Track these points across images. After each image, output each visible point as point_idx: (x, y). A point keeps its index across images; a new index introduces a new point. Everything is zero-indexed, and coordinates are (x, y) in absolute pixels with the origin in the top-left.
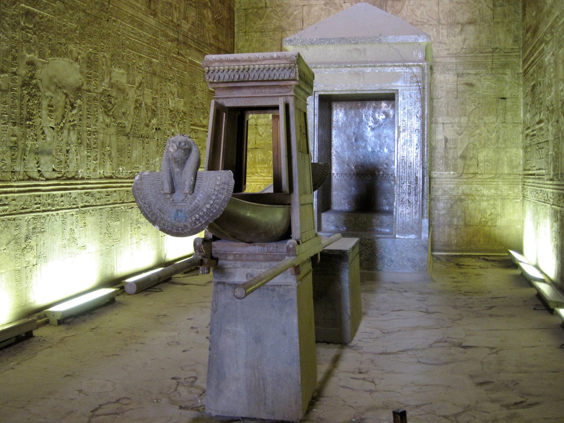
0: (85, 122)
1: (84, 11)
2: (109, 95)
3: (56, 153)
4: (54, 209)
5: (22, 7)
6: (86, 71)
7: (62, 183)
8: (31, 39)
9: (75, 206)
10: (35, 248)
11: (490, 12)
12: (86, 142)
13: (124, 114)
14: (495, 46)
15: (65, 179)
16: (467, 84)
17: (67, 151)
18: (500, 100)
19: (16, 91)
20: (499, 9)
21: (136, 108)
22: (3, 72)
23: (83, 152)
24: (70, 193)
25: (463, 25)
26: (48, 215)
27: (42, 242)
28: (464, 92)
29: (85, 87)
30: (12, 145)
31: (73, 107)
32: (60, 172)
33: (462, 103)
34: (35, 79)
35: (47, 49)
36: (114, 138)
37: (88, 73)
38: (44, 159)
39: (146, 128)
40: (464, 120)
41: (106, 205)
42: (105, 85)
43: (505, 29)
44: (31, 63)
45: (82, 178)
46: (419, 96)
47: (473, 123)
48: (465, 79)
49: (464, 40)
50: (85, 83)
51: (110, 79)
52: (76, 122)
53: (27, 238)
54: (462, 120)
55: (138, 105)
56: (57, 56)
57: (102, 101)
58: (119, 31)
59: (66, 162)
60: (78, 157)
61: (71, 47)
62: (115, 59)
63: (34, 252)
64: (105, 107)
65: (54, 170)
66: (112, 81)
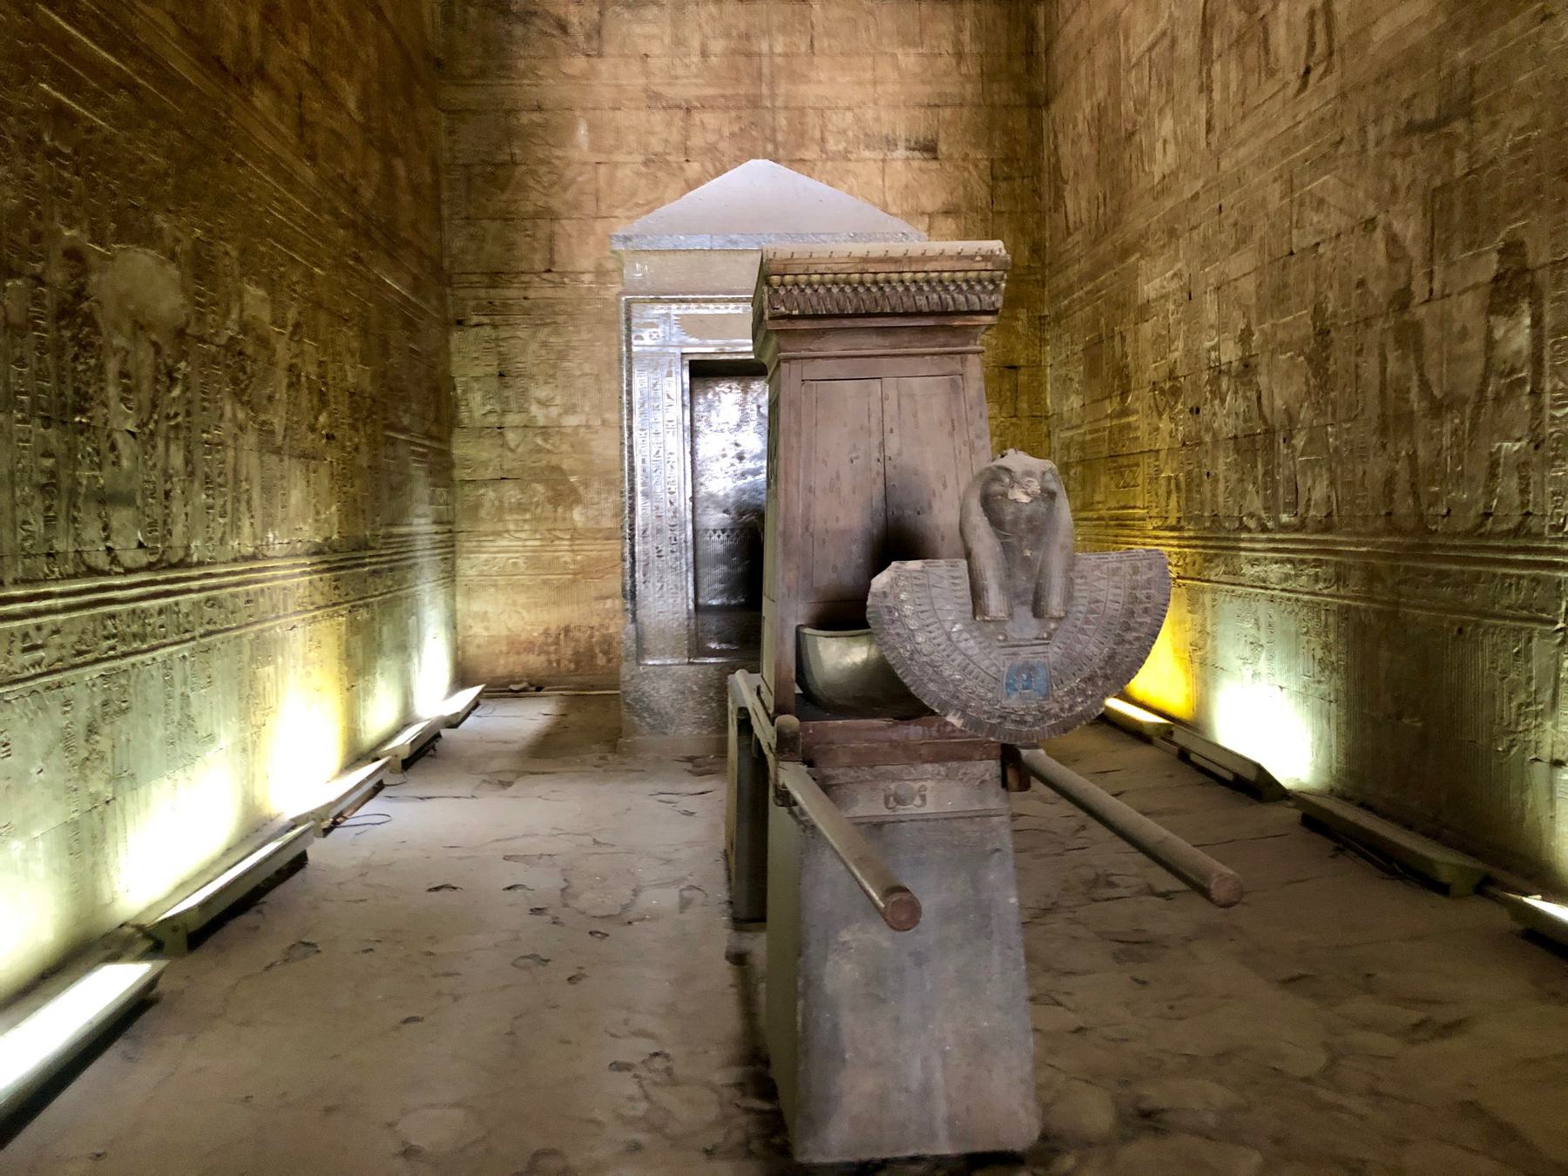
0: (196, 419)
1: (180, 129)
3: (144, 498)
4: (145, 646)
5: (46, 95)
7: (160, 577)
9: (187, 636)
10: (109, 755)
15: (164, 568)
17: (167, 494)
19: (45, 331)
20: (1003, 185)
21: (291, 385)
22: (12, 274)
23: (199, 495)
24: (177, 604)
25: (930, 215)
26: (133, 665)
27: (123, 739)
30: (44, 480)
31: (173, 381)
32: (153, 551)
37: (197, 294)
38: (120, 517)
39: (311, 436)
41: (248, 625)
50: (193, 322)
51: (242, 311)
52: (180, 419)
53: (91, 730)
57: (228, 366)
59: (165, 523)
61: (159, 219)
62: (250, 265)
63: (107, 767)
65: (141, 545)
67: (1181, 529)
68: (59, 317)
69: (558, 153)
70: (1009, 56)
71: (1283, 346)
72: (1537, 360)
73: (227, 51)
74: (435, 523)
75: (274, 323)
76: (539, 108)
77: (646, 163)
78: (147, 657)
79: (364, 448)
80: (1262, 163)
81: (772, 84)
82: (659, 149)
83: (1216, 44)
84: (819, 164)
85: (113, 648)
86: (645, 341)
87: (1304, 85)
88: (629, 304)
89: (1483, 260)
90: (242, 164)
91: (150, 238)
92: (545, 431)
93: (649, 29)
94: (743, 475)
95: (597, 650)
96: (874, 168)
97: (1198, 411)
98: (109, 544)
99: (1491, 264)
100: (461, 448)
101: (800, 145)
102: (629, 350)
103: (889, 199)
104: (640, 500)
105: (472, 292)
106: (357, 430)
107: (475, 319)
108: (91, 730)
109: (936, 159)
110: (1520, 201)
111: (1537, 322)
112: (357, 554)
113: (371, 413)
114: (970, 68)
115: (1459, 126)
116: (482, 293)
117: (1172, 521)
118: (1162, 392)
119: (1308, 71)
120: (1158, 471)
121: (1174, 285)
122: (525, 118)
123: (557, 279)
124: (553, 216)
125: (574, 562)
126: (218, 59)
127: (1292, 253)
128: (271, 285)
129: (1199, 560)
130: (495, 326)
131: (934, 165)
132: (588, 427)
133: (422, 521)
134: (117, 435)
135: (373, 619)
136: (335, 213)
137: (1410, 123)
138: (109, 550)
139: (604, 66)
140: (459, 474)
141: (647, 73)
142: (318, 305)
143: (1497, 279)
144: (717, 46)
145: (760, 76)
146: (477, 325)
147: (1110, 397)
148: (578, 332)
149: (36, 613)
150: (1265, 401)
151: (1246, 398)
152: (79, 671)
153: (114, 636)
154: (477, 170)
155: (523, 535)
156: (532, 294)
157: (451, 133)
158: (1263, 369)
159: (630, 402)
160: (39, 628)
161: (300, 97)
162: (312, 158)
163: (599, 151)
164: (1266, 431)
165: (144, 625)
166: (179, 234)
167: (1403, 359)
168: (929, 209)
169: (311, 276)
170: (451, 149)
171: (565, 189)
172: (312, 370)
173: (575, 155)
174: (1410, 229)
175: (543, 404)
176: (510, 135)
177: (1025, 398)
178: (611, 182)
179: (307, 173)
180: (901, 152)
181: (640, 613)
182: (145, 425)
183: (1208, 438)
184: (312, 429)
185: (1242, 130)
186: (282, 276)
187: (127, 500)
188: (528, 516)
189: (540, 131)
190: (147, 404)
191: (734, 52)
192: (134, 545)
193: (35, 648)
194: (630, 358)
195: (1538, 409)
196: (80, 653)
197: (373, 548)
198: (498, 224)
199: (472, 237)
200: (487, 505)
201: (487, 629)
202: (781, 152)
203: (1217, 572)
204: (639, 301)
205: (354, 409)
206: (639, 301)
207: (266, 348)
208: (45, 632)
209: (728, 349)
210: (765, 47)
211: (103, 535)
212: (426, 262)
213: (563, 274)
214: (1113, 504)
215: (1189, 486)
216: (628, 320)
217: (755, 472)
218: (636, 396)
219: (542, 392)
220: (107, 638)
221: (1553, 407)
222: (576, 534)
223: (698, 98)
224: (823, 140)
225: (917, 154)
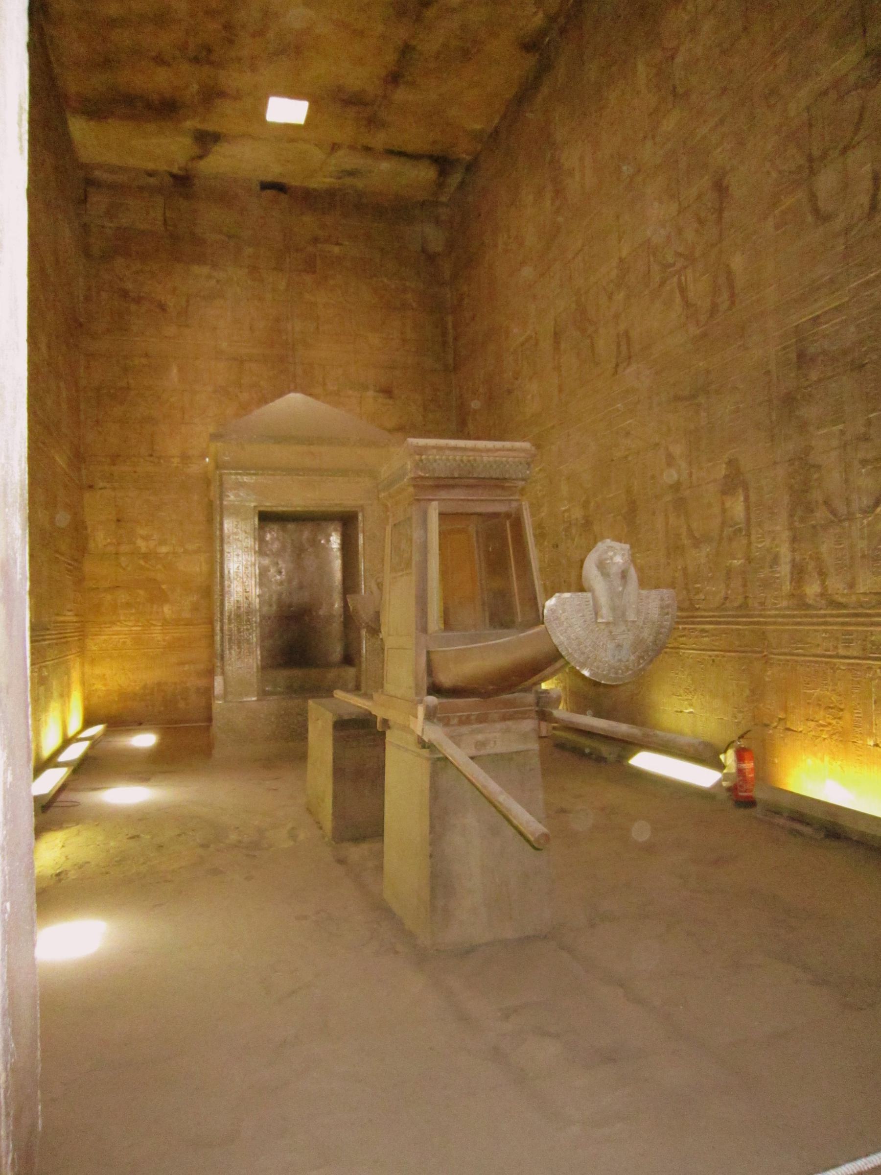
11: (421, 418)
72: (748, 520)
74: (76, 615)
76: (147, 355)
83: (563, 346)
86: (231, 497)
88: (221, 476)
92: (146, 557)
94: (281, 583)
95: (179, 697)
97: (557, 546)
100: (89, 567)
102: (221, 504)
107: (101, 485)
109: (391, 397)
119: (617, 365)
122: (137, 362)
125: (164, 640)
127: (612, 460)
130: (114, 489)
131: (391, 402)
132: (174, 553)
133: (70, 613)
143: (726, 476)
146: (101, 489)
155: (130, 624)
175: (146, 538)
180: (371, 393)
181: (228, 668)
188: (133, 611)
195: (750, 543)
197: (48, 629)
201: (105, 685)
204: (227, 474)
206: (227, 474)
209: (283, 503)
213: (159, 458)
217: (290, 581)
219: (142, 532)
222: (165, 623)
224: (325, 384)
225: (381, 395)
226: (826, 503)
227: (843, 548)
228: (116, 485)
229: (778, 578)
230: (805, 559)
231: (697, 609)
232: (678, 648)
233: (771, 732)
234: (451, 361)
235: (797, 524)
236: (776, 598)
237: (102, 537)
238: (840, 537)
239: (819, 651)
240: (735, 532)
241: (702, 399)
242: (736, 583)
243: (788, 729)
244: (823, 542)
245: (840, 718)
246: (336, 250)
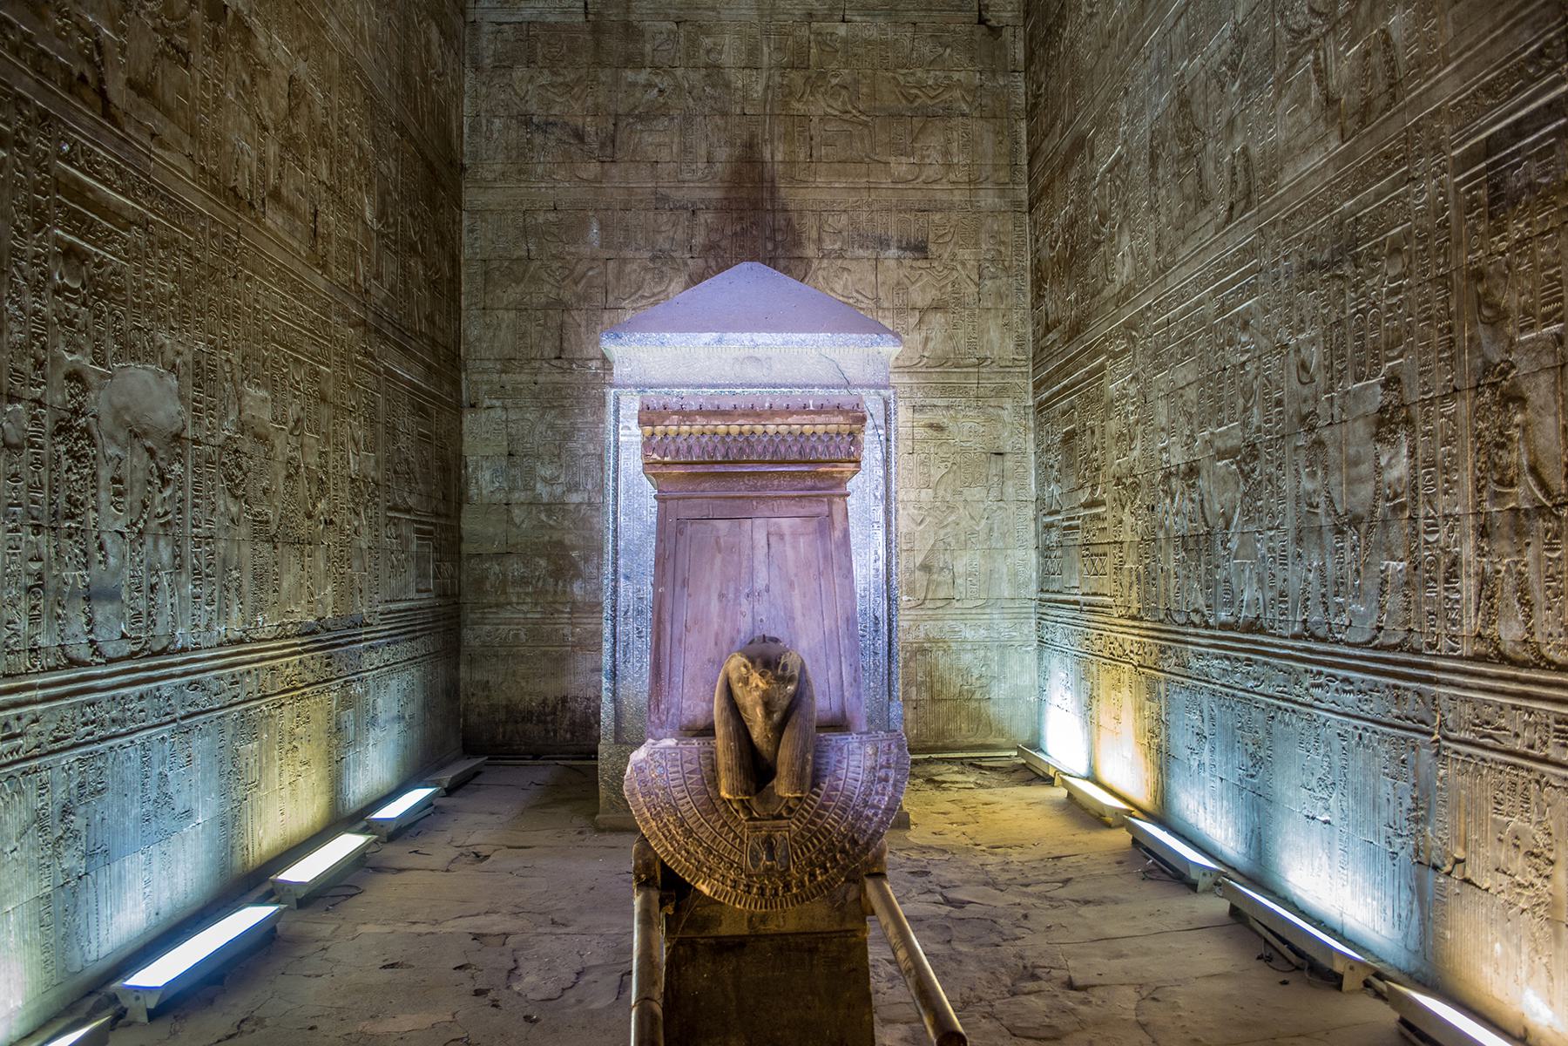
2: (236, 451)
6: (192, 394)
8: (76, 316)
9: (168, 718)
11: (973, 289)
12: (191, 561)
13: (265, 491)
14: (982, 355)
16: (931, 426)
17: (152, 588)
18: (994, 458)
20: (989, 283)
21: (289, 476)
23: (184, 585)
28: (924, 441)
29: (189, 433)
31: (165, 483)
33: (922, 463)
34: (84, 414)
35: (110, 342)
36: (246, 550)
39: (307, 523)
40: (926, 495)
41: (231, 705)
42: (228, 428)
43: (1000, 322)
44: (75, 376)
45: (184, 650)
46: (879, 456)
47: (944, 501)
48: (928, 417)
49: (927, 339)
53: (66, 811)
54: (923, 494)
55: (292, 471)
56: (133, 359)
57: (224, 464)
58: (257, 301)
59: (149, 614)
60: (176, 600)
61: (162, 337)
64: (230, 478)
65: (124, 636)
66: (244, 417)
67: (1141, 619)
68: (53, 435)
69: (573, 250)
70: (996, 168)
71: (1221, 455)
73: (242, 182)
74: (438, 596)
75: (275, 420)
77: (653, 259)
78: (124, 741)
79: (365, 531)
80: (1201, 283)
81: (773, 189)
82: (667, 246)
83: (1161, 172)
84: (816, 262)
85: (92, 734)
87: (1229, 220)
88: (617, 399)
89: (1369, 392)
90: (248, 278)
91: (153, 353)
92: (549, 508)
93: (658, 139)
96: (867, 265)
98: (92, 637)
99: (1377, 397)
100: (470, 523)
101: (798, 244)
102: (617, 441)
103: (881, 294)
104: (622, 582)
105: (485, 377)
106: (358, 514)
107: (487, 402)
108: (66, 811)
110: (1399, 341)
111: (1412, 454)
112: (350, 632)
113: (373, 495)
114: (959, 175)
115: (1347, 269)
116: (495, 377)
117: (1134, 611)
118: (1125, 488)
120: (1123, 562)
121: (1132, 390)
123: (566, 366)
124: (562, 306)
126: (234, 189)
128: (272, 385)
129: (1155, 650)
130: (505, 408)
132: (590, 504)
134: (104, 536)
135: (367, 693)
136: (345, 314)
137: (1310, 262)
138: (92, 642)
139: (614, 170)
140: (466, 548)
141: (656, 178)
142: (324, 399)
143: (1383, 410)
144: (722, 154)
145: (762, 180)
147: (1081, 487)
148: (583, 414)
149: (16, 705)
150: (1206, 505)
151: (1192, 500)
152: (58, 756)
153: (93, 722)
154: (495, 264)
155: (525, 608)
156: (541, 379)
157: (471, 231)
158: (1204, 473)
159: (616, 489)
160: (19, 718)
161: (315, 215)
162: (324, 267)
163: (609, 247)
164: (1208, 533)
165: (123, 711)
166: (180, 348)
167: (1313, 475)
168: (920, 305)
169: (317, 373)
170: (472, 245)
171: (576, 284)
172: (313, 460)
173: (585, 251)
174: (1315, 356)
176: (525, 232)
177: (1010, 483)
178: (619, 276)
179: (320, 281)
180: (893, 252)
181: (621, 692)
182: (135, 524)
183: (1161, 535)
184: (310, 516)
185: (1183, 252)
186: (285, 376)
187: (113, 596)
189: (554, 230)
190: (137, 505)
191: (740, 160)
192: (118, 636)
193: (14, 736)
194: (617, 447)
196: (57, 740)
197: (368, 625)
198: (512, 314)
199: (488, 326)
200: (492, 578)
202: (780, 251)
203: (1170, 663)
205: (356, 494)
207: (264, 444)
208: (25, 721)
210: (768, 156)
211: (86, 629)
212: (441, 351)
213: (571, 361)
214: (1086, 590)
215: (1147, 578)
216: (617, 411)
218: (621, 486)
220: (85, 724)
221: (1426, 532)
223: (703, 201)
224: (820, 240)
225: (908, 254)
226: (1534, 470)
227: (1559, 559)
228: (509, 402)
229: (1457, 601)
230: (1498, 572)
231: (1337, 642)
232: (1311, 706)
233: (1441, 880)
234: (1025, 197)
235: (1487, 505)
236: (1453, 637)
237: (488, 477)
238: (1556, 537)
239: (1519, 745)
240: (1394, 508)
241: (1347, 269)
242: (1394, 601)
243: (1467, 881)
244: (1528, 544)
245: (1547, 877)
246: (842, 30)
